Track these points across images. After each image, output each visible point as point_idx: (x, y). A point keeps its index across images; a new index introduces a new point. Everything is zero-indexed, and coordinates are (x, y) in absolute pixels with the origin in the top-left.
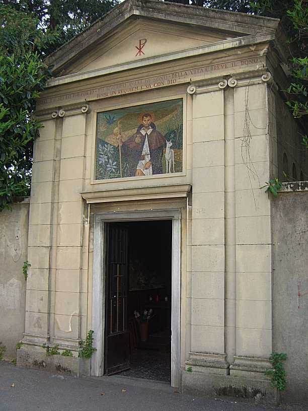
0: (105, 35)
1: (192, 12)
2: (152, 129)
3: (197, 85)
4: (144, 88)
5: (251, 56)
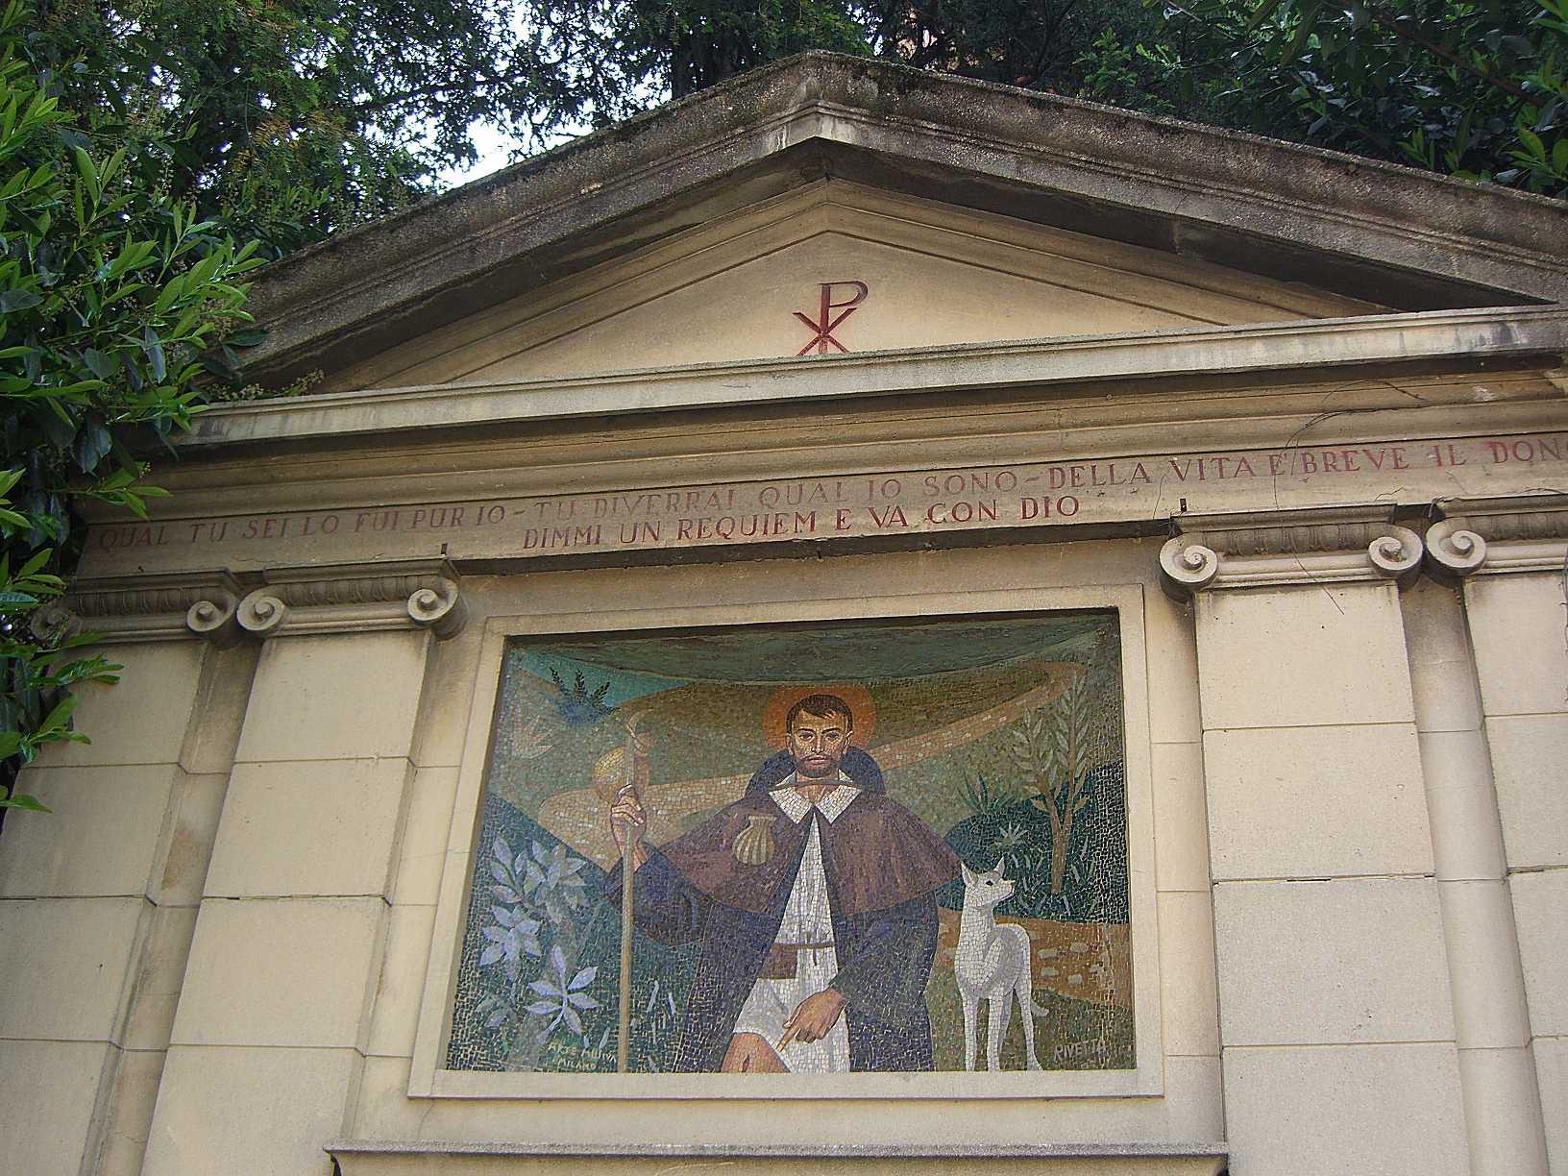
0: (623, 223)
1: (1204, 157)
2: (855, 791)
3: (1219, 538)
4: (861, 526)
5: (1550, 420)
